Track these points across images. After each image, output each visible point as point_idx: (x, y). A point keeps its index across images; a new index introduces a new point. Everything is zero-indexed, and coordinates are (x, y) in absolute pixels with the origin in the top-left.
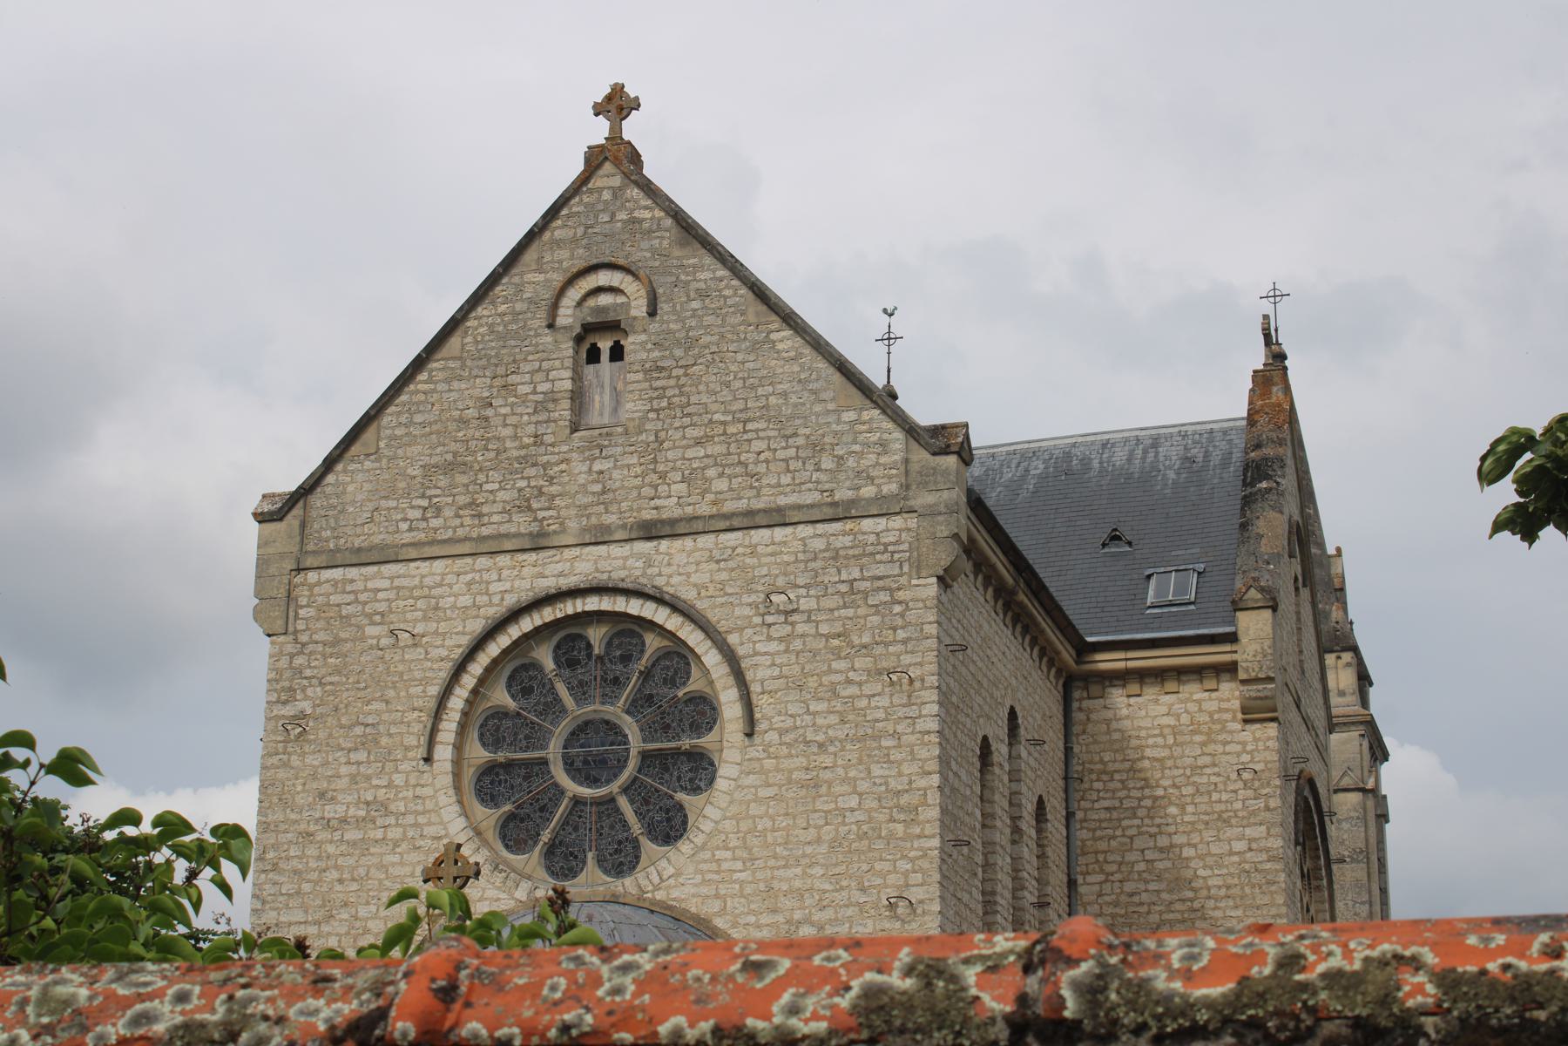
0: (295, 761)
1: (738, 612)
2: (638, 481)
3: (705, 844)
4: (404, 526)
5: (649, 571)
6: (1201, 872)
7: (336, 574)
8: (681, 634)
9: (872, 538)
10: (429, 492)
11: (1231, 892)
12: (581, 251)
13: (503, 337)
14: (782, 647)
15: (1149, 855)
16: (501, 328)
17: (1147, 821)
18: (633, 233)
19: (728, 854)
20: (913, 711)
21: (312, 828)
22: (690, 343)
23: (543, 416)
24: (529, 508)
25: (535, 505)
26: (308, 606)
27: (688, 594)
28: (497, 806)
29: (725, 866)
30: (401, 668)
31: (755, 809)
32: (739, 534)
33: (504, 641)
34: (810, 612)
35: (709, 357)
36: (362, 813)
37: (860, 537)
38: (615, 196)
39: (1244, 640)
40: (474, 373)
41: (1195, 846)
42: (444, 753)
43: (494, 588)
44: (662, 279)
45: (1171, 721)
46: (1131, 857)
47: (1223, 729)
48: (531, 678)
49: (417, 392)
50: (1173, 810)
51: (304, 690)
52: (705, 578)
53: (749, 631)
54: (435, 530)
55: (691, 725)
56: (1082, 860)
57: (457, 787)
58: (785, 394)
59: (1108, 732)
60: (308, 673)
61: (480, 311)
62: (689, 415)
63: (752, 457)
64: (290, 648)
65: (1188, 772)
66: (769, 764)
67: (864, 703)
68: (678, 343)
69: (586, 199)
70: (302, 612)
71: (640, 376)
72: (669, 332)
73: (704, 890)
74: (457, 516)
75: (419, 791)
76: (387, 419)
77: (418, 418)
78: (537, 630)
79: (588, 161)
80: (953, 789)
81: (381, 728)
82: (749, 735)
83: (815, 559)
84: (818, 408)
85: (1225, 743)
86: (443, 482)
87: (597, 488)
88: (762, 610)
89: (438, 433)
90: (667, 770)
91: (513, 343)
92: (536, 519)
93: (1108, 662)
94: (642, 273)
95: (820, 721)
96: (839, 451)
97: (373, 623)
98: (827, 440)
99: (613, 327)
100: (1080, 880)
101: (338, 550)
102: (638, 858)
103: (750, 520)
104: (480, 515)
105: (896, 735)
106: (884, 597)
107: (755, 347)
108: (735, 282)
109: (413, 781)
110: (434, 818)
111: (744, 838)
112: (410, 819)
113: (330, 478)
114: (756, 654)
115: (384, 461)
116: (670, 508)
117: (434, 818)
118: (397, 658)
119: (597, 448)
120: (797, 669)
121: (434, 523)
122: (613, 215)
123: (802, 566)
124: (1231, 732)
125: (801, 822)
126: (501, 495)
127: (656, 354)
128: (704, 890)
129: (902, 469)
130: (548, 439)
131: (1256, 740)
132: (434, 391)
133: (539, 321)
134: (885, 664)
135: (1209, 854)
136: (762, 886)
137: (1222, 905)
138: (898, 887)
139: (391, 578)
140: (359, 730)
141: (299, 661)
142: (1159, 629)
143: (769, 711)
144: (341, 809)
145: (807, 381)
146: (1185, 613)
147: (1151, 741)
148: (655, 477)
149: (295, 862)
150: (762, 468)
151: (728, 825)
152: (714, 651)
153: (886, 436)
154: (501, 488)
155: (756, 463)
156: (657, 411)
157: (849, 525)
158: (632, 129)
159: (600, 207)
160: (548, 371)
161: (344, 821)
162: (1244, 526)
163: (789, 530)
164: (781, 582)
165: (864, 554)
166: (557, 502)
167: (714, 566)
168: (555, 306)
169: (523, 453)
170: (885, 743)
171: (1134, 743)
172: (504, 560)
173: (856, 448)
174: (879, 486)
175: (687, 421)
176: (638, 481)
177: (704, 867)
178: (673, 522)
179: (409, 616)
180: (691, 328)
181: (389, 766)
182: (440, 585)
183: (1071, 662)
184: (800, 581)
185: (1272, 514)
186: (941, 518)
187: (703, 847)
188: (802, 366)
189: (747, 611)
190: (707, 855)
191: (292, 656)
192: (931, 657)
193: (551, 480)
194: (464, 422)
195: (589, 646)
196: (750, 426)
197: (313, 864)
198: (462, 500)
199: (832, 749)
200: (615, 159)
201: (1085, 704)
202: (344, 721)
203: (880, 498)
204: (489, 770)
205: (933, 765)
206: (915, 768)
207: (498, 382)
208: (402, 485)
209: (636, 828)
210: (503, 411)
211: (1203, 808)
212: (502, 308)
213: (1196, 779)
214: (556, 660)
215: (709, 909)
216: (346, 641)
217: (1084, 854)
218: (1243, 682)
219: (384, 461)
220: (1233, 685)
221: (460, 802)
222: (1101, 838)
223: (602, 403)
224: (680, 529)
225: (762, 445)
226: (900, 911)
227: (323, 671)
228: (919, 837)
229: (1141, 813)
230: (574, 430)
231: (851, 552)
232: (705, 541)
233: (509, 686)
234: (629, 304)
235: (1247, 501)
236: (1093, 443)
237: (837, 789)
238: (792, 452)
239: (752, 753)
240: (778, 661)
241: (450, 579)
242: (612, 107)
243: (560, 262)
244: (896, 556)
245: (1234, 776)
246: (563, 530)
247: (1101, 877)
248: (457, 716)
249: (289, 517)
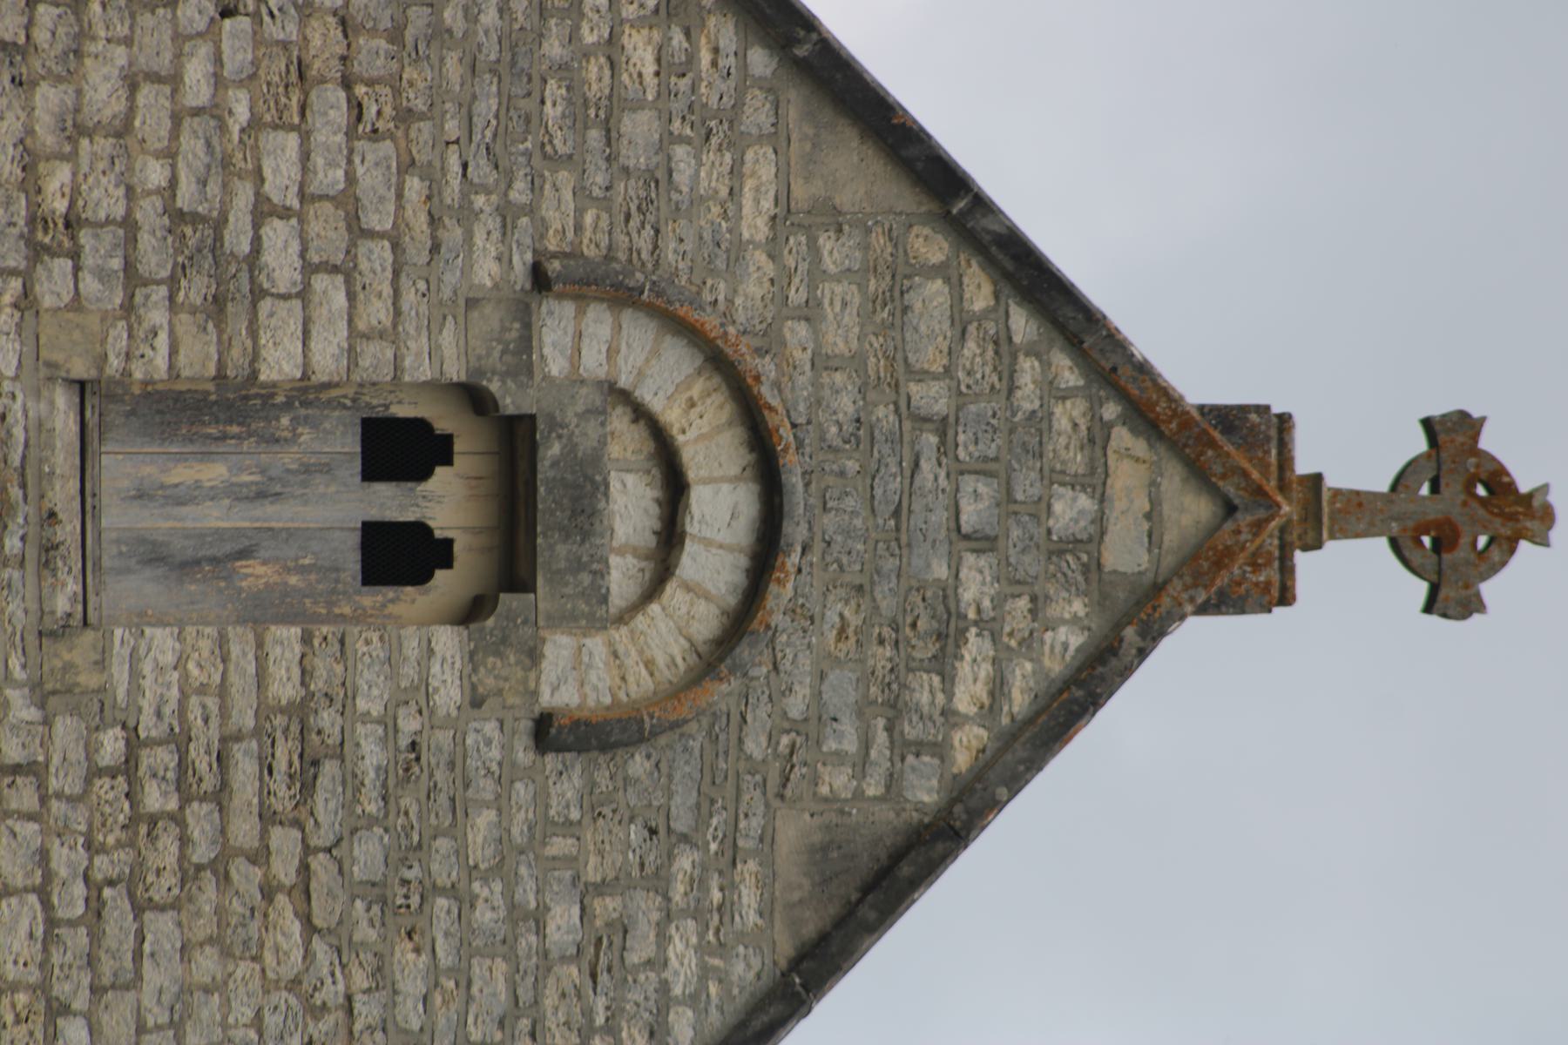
12: (846, 404)
16: (554, 48)
22: (399, 905)
23: (153, 256)
35: (331, 993)
38: (1073, 544)
44: (685, 768)
62: (96, 908)
69: (1069, 415)
71: (284, 688)
72: (460, 809)
79: (1230, 419)
91: (487, 107)
94: (722, 693)
99: (513, 569)
122: (983, 542)
127: (372, 755)
133: (565, 217)
156: (128, 766)
158: (1353, 578)
159: (1026, 486)
160: (347, 271)
168: (612, 286)
175: (72, 900)
180: (465, 902)
200: (1244, 507)
207: (323, 40)
210: (196, 72)
212: (641, 51)
223: (180, 498)
230: (82, 387)
234: (596, 624)
243: (810, 313)
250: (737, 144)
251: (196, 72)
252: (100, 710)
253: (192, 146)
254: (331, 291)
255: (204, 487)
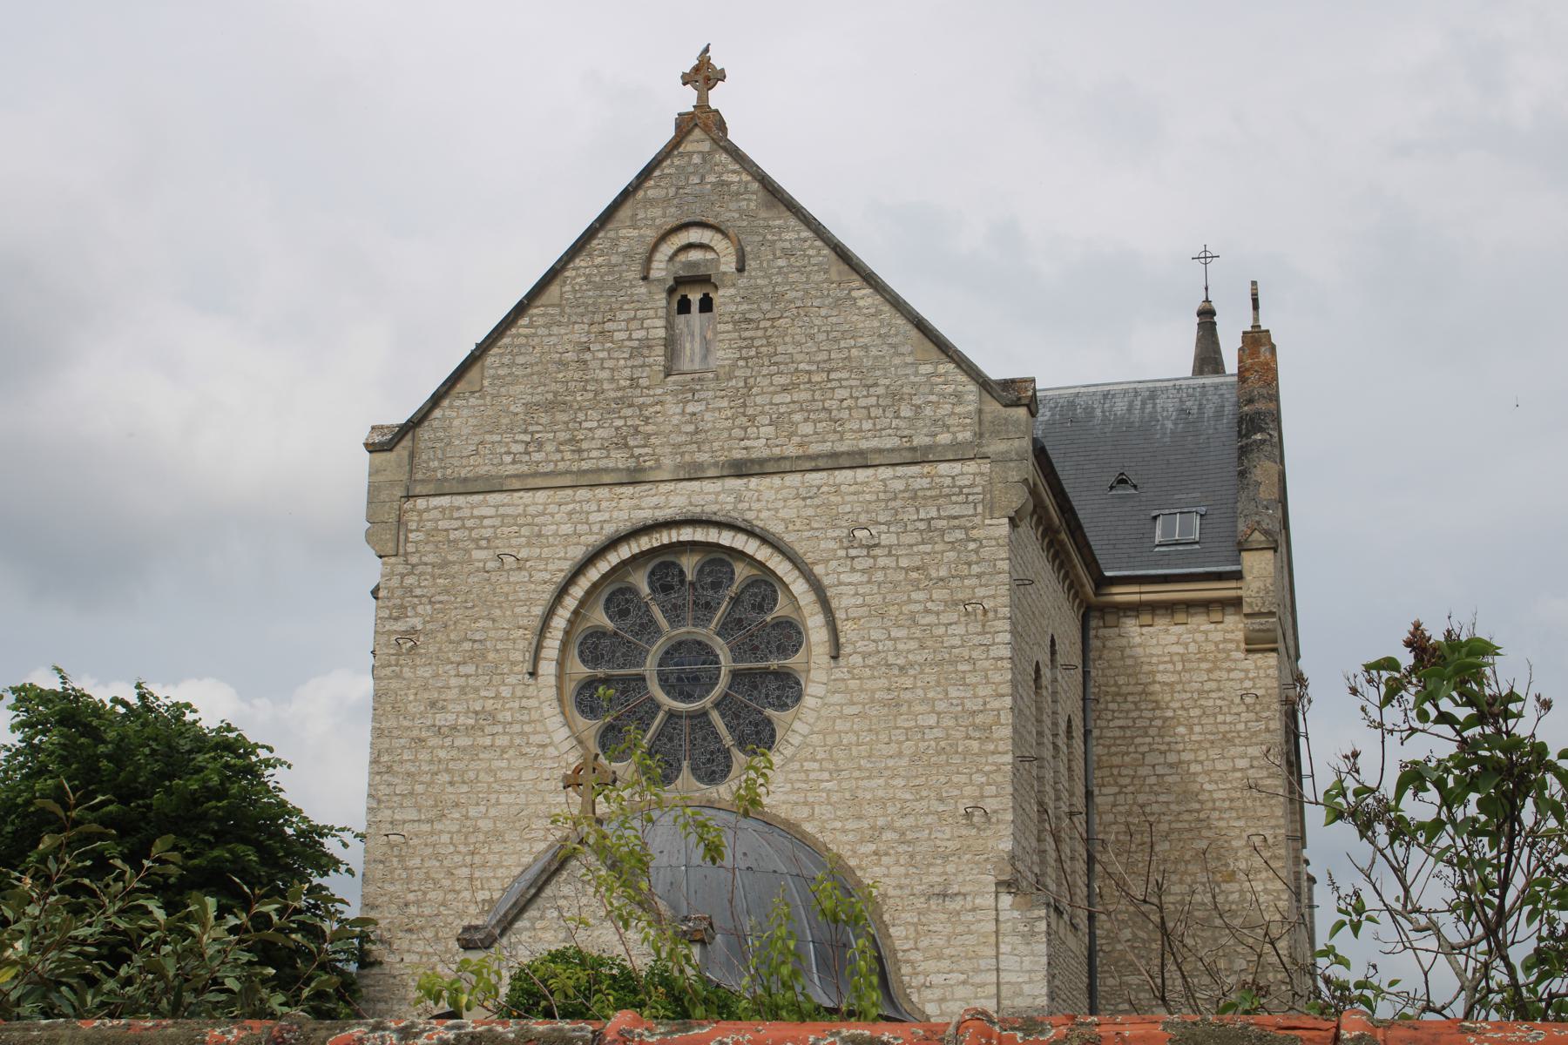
0: (407, 672)
1: (823, 545)
2: (729, 423)
3: (794, 756)
4: (508, 459)
5: (740, 506)
6: (1207, 786)
7: (444, 501)
8: (770, 564)
9: (948, 481)
10: (531, 429)
11: (1235, 804)
12: (673, 210)
13: (599, 287)
14: (865, 578)
15: (1160, 770)
17: (1157, 739)
18: (721, 195)
19: (816, 765)
20: (987, 639)
21: (424, 734)
22: (776, 298)
23: (639, 361)
24: (626, 445)
25: (631, 443)
26: (417, 530)
27: (776, 528)
28: (596, 717)
29: (812, 776)
30: (506, 589)
31: (840, 725)
32: (824, 474)
33: (603, 567)
34: (890, 547)
36: (472, 722)
37: (937, 480)
39: (1248, 578)
40: (574, 319)
41: (1201, 763)
42: (548, 668)
43: (592, 518)
45: (1180, 649)
46: (1142, 771)
47: (1228, 658)
48: (627, 601)
49: (519, 335)
50: (1181, 730)
51: (414, 608)
52: (792, 514)
53: (834, 563)
54: (538, 463)
55: (778, 648)
56: (1098, 773)
57: (560, 700)
58: (865, 347)
59: (1123, 658)
60: (418, 592)
61: (578, 262)
62: (776, 364)
63: (835, 404)
64: (401, 569)
65: (1195, 696)
66: (853, 684)
67: (941, 630)
68: (765, 297)
69: (677, 162)
70: (412, 536)
71: (730, 327)
72: (757, 287)
73: (794, 798)
74: (558, 451)
75: (524, 702)
76: (491, 359)
77: (520, 360)
78: (634, 558)
79: (678, 126)
80: (1020, 711)
81: (488, 644)
82: (835, 658)
83: (895, 499)
84: (897, 361)
85: (1230, 670)
86: (545, 419)
87: (691, 428)
88: (846, 543)
89: (539, 373)
90: (756, 687)
92: (632, 456)
93: (1122, 594)
94: (731, 232)
95: (900, 646)
96: (917, 401)
97: (479, 548)
98: (905, 390)
99: (704, 280)
100: (1096, 792)
101: (445, 479)
102: (729, 767)
103: (834, 462)
104: (580, 451)
105: (971, 660)
106: (960, 535)
107: (837, 303)
108: (819, 243)
109: (519, 694)
110: (539, 728)
111: (831, 752)
112: (517, 728)
113: (437, 413)
114: (840, 584)
115: (488, 398)
116: (759, 449)
117: (539, 728)
118: (503, 580)
119: (689, 392)
120: (879, 599)
121: (537, 457)
122: (703, 178)
123: (883, 505)
124: (1235, 661)
125: (884, 737)
126: (599, 433)
127: (745, 307)
128: (794, 798)
129: (976, 419)
130: (644, 382)
131: (1257, 668)
132: (535, 335)
133: (633, 273)
134: (960, 596)
135: (1214, 770)
136: (847, 795)
137: (1226, 816)
138: (974, 798)
139: (496, 507)
140: (467, 646)
141: (409, 581)
142: (1168, 566)
143: (853, 636)
144: (451, 718)
145: (887, 335)
146: (1191, 552)
147: (1161, 667)
148: (745, 419)
149: (408, 766)
150: (845, 414)
151: (815, 739)
152: (801, 581)
153: (960, 388)
154: (599, 427)
155: (839, 410)
156: (746, 359)
157: (927, 468)
158: (718, 98)
159: (691, 169)
161: (454, 728)
162: (1242, 474)
163: (870, 471)
164: (863, 518)
165: (941, 495)
166: (653, 440)
167: (802, 503)
168: (649, 260)
169: (619, 394)
170: (961, 667)
171: (1146, 668)
172: (602, 492)
173: (933, 398)
174: (954, 433)
175: (774, 369)
176: (729, 423)
177: (793, 776)
178: (762, 462)
179: (513, 542)
181: (497, 679)
182: (543, 514)
183: (1091, 593)
184: (881, 519)
185: (1268, 464)
186: (1012, 464)
187: (792, 759)
188: (881, 321)
189: (832, 545)
190: (796, 766)
191: (403, 576)
192: (1004, 590)
193: (647, 420)
194: (563, 364)
195: (682, 572)
196: (833, 376)
197: (425, 768)
198: (563, 436)
199: (911, 672)
200: (700, 124)
201: (1102, 632)
202: (453, 636)
203: (955, 445)
204: (589, 684)
205: (1006, 689)
206: (989, 690)
207: (595, 328)
208: (505, 421)
209: (728, 740)
210: (601, 355)
211: (1209, 728)
212: (599, 260)
213: (1202, 702)
214: (651, 584)
215: (799, 815)
216: (454, 563)
217: (1100, 768)
218: (1247, 616)
219: (488, 398)
220: (1237, 618)
221: (563, 713)
222: (1115, 754)
223: (693, 353)
224: (769, 468)
225: (844, 393)
226: (975, 819)
227: (433, 590)
228: (993, 753)
229: (1152, 731)
230: (668, 375)
231: (928, 493)
232: (793, 480)
233: (607, 609)
234: (718, 260)
235: (1243, 451)
236: (1094, 393)
237: (918, 708)
238: (873, 400)
239: (837, 674)
240: (861, 591)
241: (552, 508)
242: (700, 78)
243: (653, 219)
244: (971, 498)
245: (1237, 700)
246: (659, 467)
247: (1116, 789)
248: (560, 635)
249: (399, 447)
250: (618, 239)
251: (601, 355)
252: (734, 366)
253: (616, 355)
254: (647, 323)
255: (690, 350)
